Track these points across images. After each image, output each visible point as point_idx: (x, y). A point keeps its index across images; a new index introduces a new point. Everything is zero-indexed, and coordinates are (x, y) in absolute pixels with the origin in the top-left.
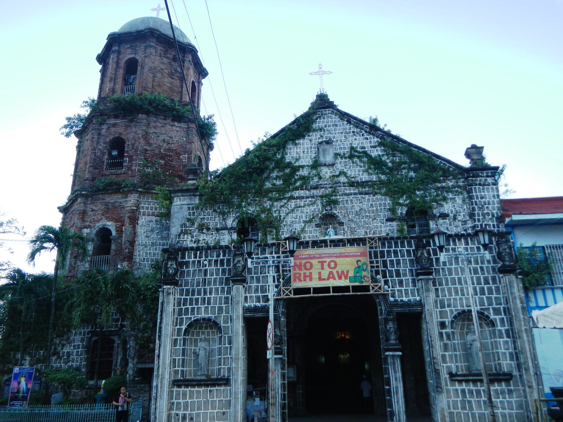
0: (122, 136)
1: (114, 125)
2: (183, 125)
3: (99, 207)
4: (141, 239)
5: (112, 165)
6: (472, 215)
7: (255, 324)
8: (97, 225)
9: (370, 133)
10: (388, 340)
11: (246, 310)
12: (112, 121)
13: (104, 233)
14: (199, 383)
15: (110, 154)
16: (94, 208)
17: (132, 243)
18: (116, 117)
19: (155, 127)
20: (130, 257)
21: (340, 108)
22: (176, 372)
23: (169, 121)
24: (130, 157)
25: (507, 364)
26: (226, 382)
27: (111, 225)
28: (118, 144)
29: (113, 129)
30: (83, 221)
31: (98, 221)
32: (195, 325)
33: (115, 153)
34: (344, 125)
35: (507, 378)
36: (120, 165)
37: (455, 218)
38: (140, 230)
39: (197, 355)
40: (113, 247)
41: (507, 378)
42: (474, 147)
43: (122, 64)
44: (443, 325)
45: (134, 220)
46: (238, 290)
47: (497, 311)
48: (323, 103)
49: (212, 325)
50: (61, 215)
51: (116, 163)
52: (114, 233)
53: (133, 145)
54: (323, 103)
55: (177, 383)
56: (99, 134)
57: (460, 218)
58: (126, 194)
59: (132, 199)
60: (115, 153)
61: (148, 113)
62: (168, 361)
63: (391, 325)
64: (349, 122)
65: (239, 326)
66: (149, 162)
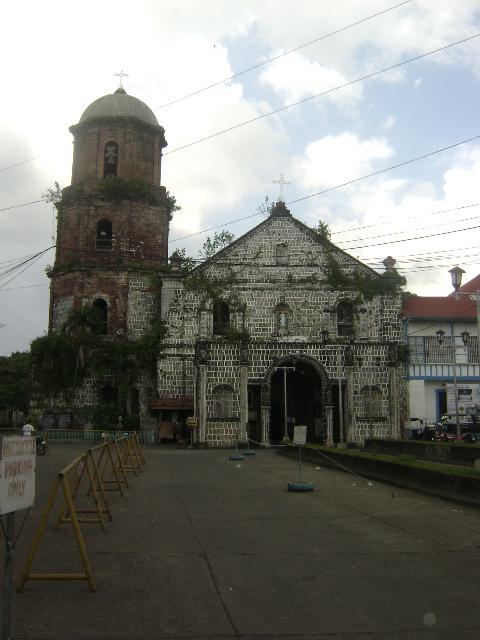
0: (109, 218)
1: (101, 207)
2: (157, 208)
3: (93, 281)
4: (132, 310)
5: (100, 244)
6: (382, 311)
7: (254, 390)
8: (94, 296)
9: (316, 241)
10: (326, 399)
11: (250, 381)
12: (100, 204)
13: (100, 303)
14: (222, 420)
15: (99, 236)
16: (91, 281)
17: (125, 314)
18: (103, 199)
19: (137, 211)
20: (124, 325)
21: (295, 216)
22: (208, 414)
23: (147, 204)
24: (118, 239)
25: (384, 413)
26: (238, 420)
27: (105, 297)
28: (105, 225)
29: (100, 210)
30: (82, 292)
31: (95, 293)
32: (218, 389)
33: (103, 233)
34: (297, 232)
35: (383, 419)
36: (109, 244)
37: (371, 312)
38: (131, 303)
39: (219, 405)
40: (109, 314)
41: (383, 419)
42: (390, 258)
43: (103, 144)
44: (356, 393)
45: (125, 295)
46: (243, 370)
47: (384, 386)
48: (280, 211)
49: (228, 388)
50: (49, 281)
51: (105, 243)
52: (109, 304)
53: (120, 227)
54: (280, 211)
55: (208, 419)
56: (89, 215)
57: (374, 312)
58: (117, 271)
59: (122, 278)
60: (103, 233)
61: (130, 198)
62: (205, 405)
63: (329, 392)
64: (301, 229)
65: (246, 391)
66: (132, 243)
